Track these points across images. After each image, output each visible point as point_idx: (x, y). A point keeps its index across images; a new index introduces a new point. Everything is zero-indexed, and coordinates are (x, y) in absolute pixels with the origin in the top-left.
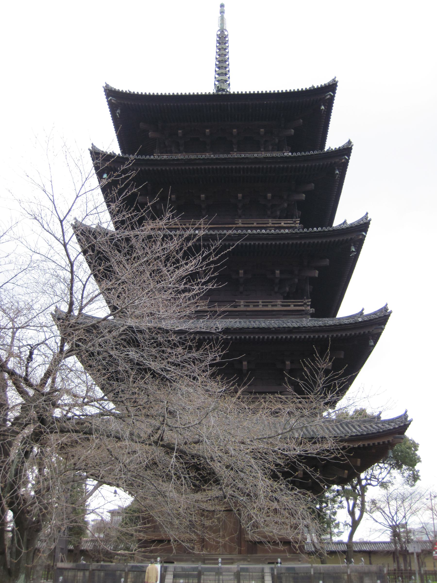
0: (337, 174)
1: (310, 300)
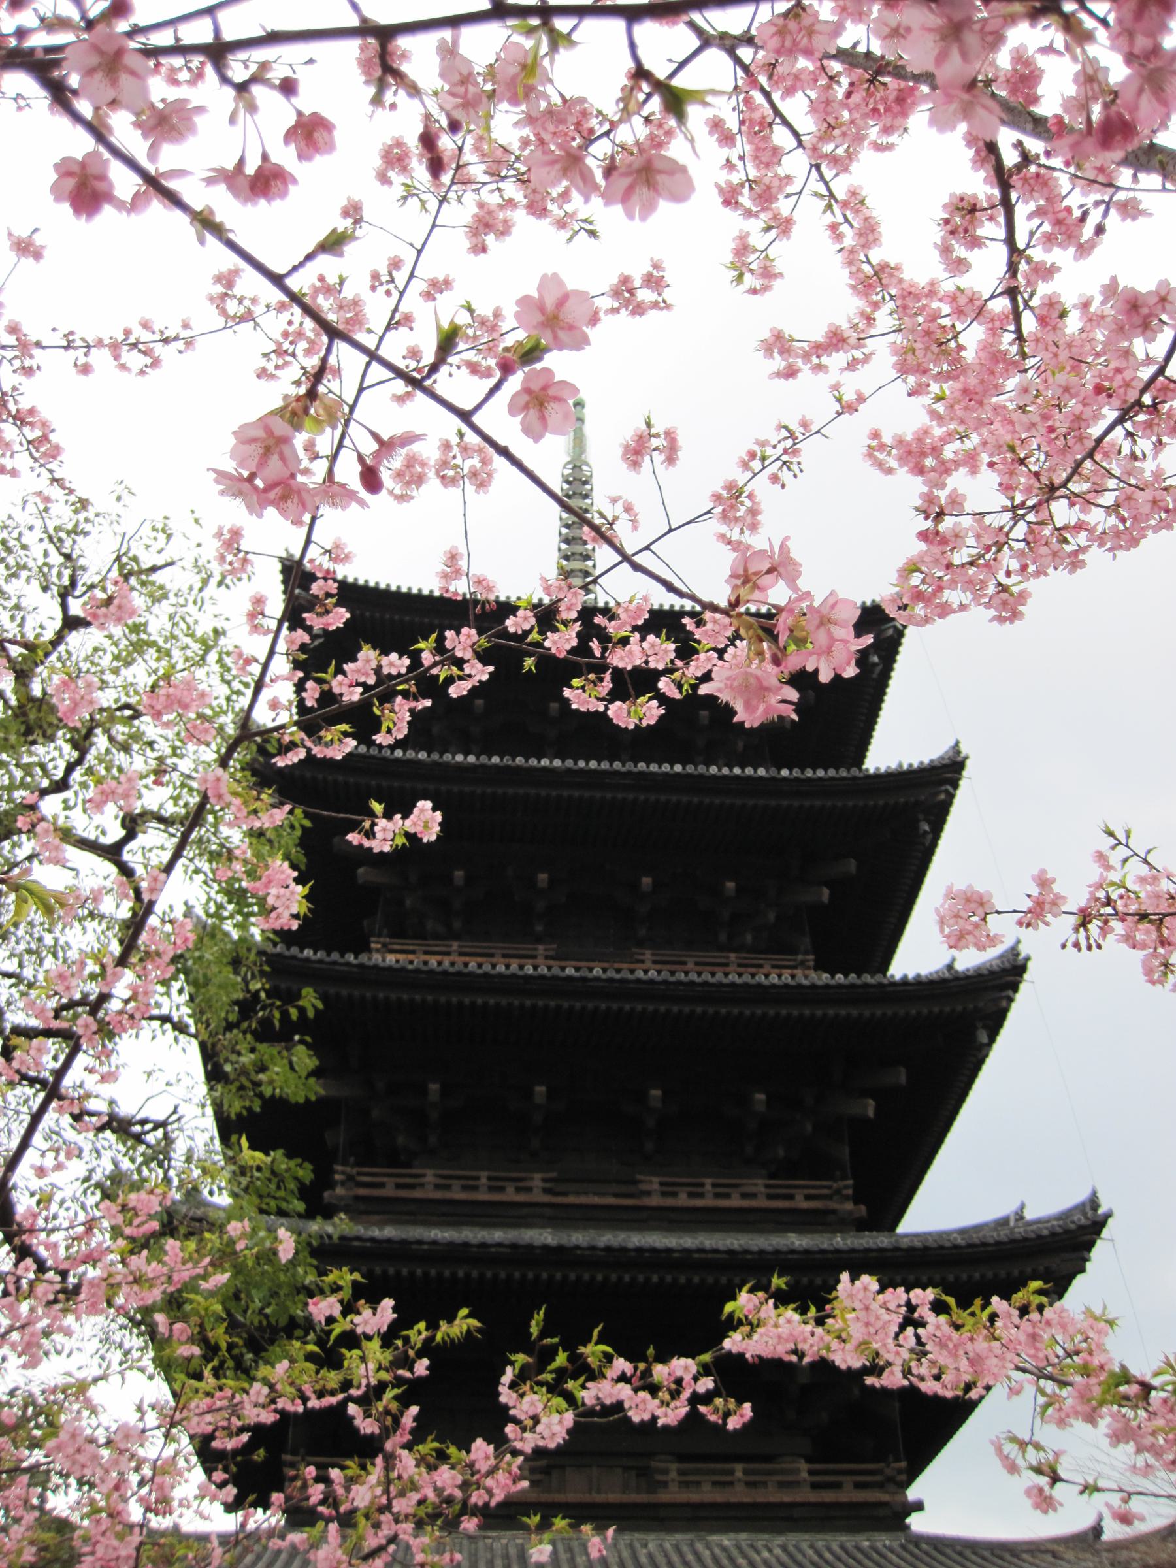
0: (925, 832)
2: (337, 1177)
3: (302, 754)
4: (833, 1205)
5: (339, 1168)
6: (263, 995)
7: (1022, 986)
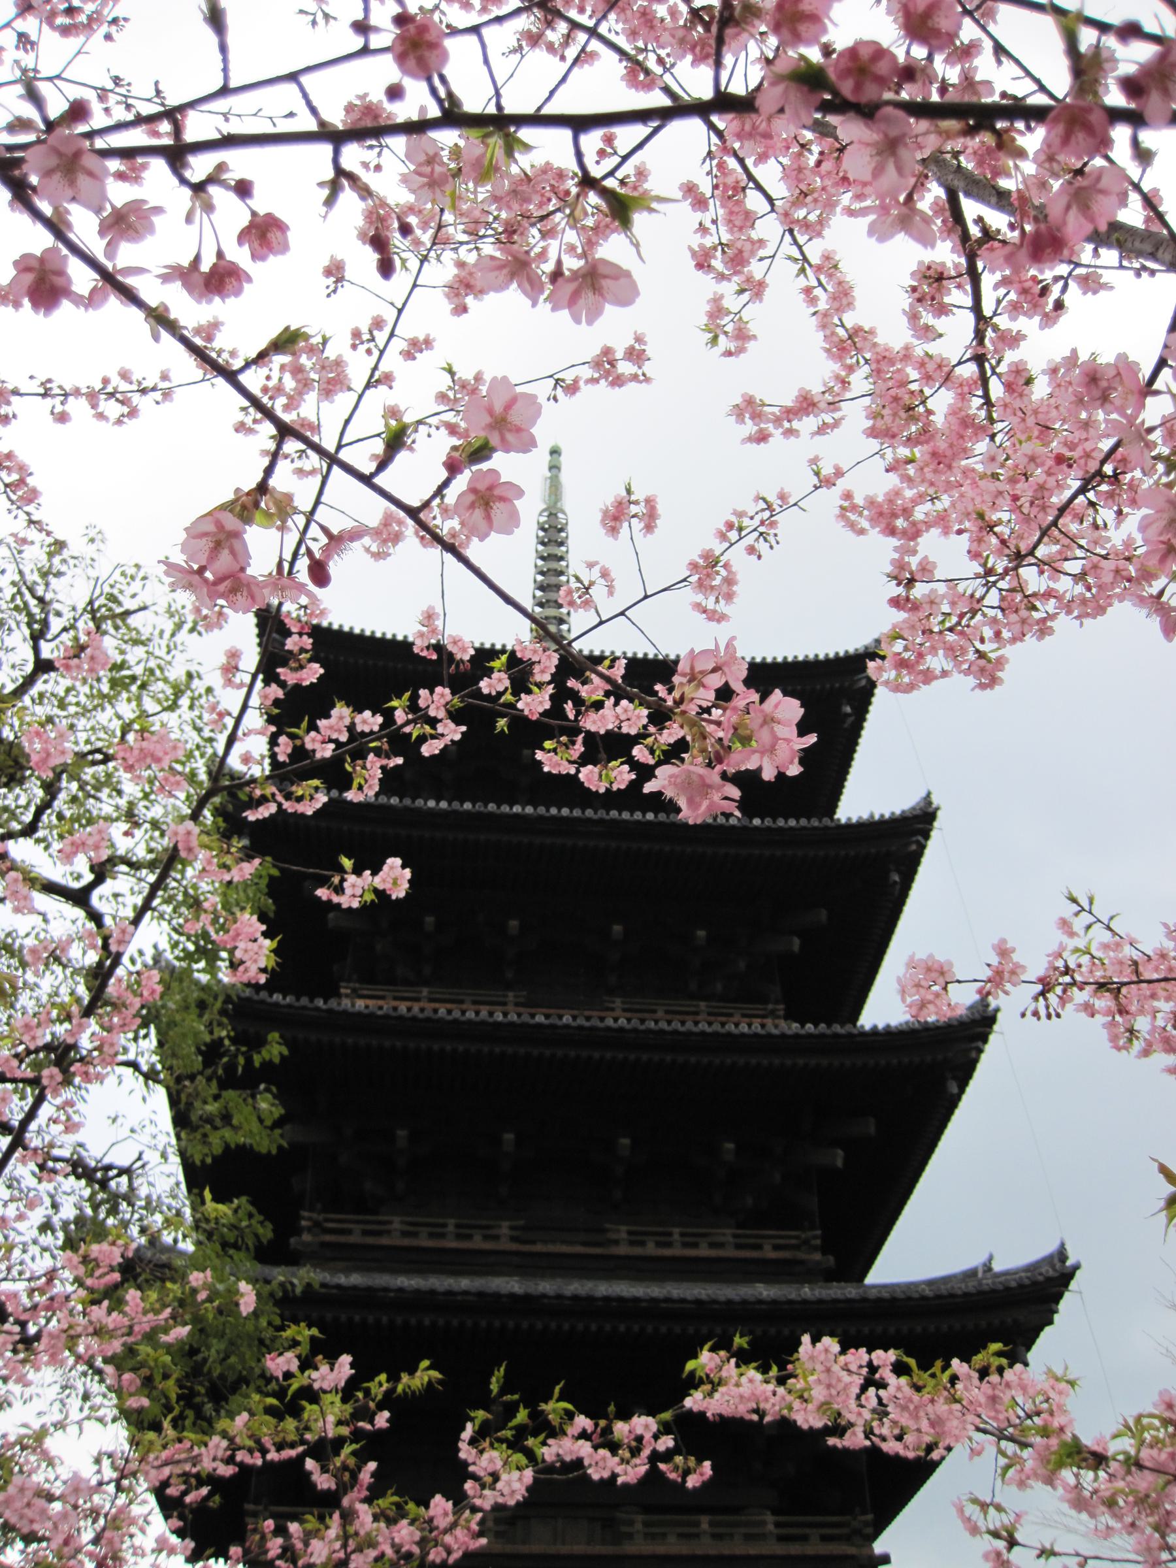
1: (819, 1232)
2: (304, 1223)
3: (272, 808)
4: (801, 1255)
5: (306, 1214)
6: (227, 1042)
7: (992, 1037)
